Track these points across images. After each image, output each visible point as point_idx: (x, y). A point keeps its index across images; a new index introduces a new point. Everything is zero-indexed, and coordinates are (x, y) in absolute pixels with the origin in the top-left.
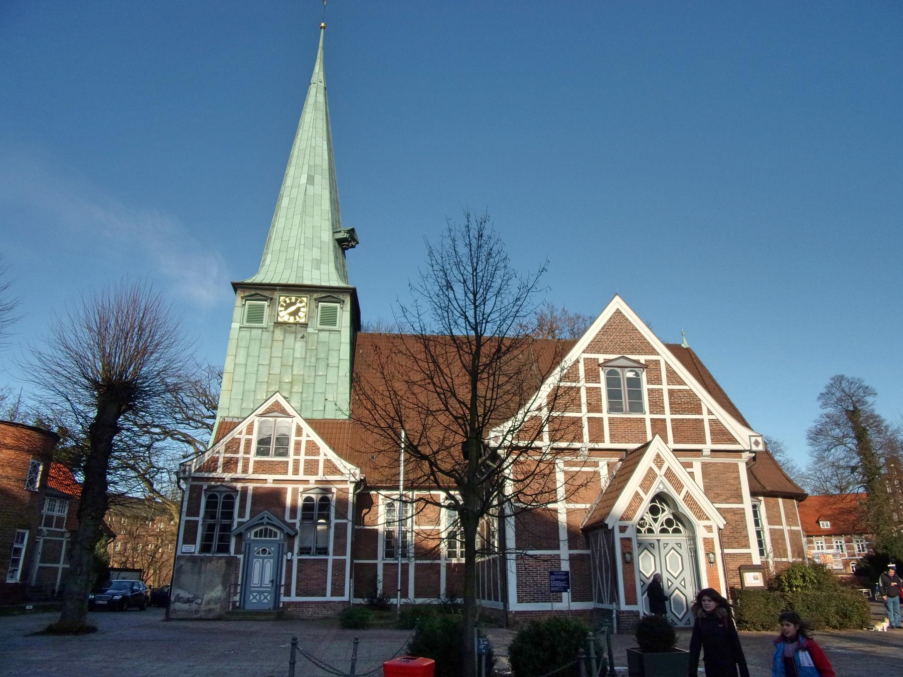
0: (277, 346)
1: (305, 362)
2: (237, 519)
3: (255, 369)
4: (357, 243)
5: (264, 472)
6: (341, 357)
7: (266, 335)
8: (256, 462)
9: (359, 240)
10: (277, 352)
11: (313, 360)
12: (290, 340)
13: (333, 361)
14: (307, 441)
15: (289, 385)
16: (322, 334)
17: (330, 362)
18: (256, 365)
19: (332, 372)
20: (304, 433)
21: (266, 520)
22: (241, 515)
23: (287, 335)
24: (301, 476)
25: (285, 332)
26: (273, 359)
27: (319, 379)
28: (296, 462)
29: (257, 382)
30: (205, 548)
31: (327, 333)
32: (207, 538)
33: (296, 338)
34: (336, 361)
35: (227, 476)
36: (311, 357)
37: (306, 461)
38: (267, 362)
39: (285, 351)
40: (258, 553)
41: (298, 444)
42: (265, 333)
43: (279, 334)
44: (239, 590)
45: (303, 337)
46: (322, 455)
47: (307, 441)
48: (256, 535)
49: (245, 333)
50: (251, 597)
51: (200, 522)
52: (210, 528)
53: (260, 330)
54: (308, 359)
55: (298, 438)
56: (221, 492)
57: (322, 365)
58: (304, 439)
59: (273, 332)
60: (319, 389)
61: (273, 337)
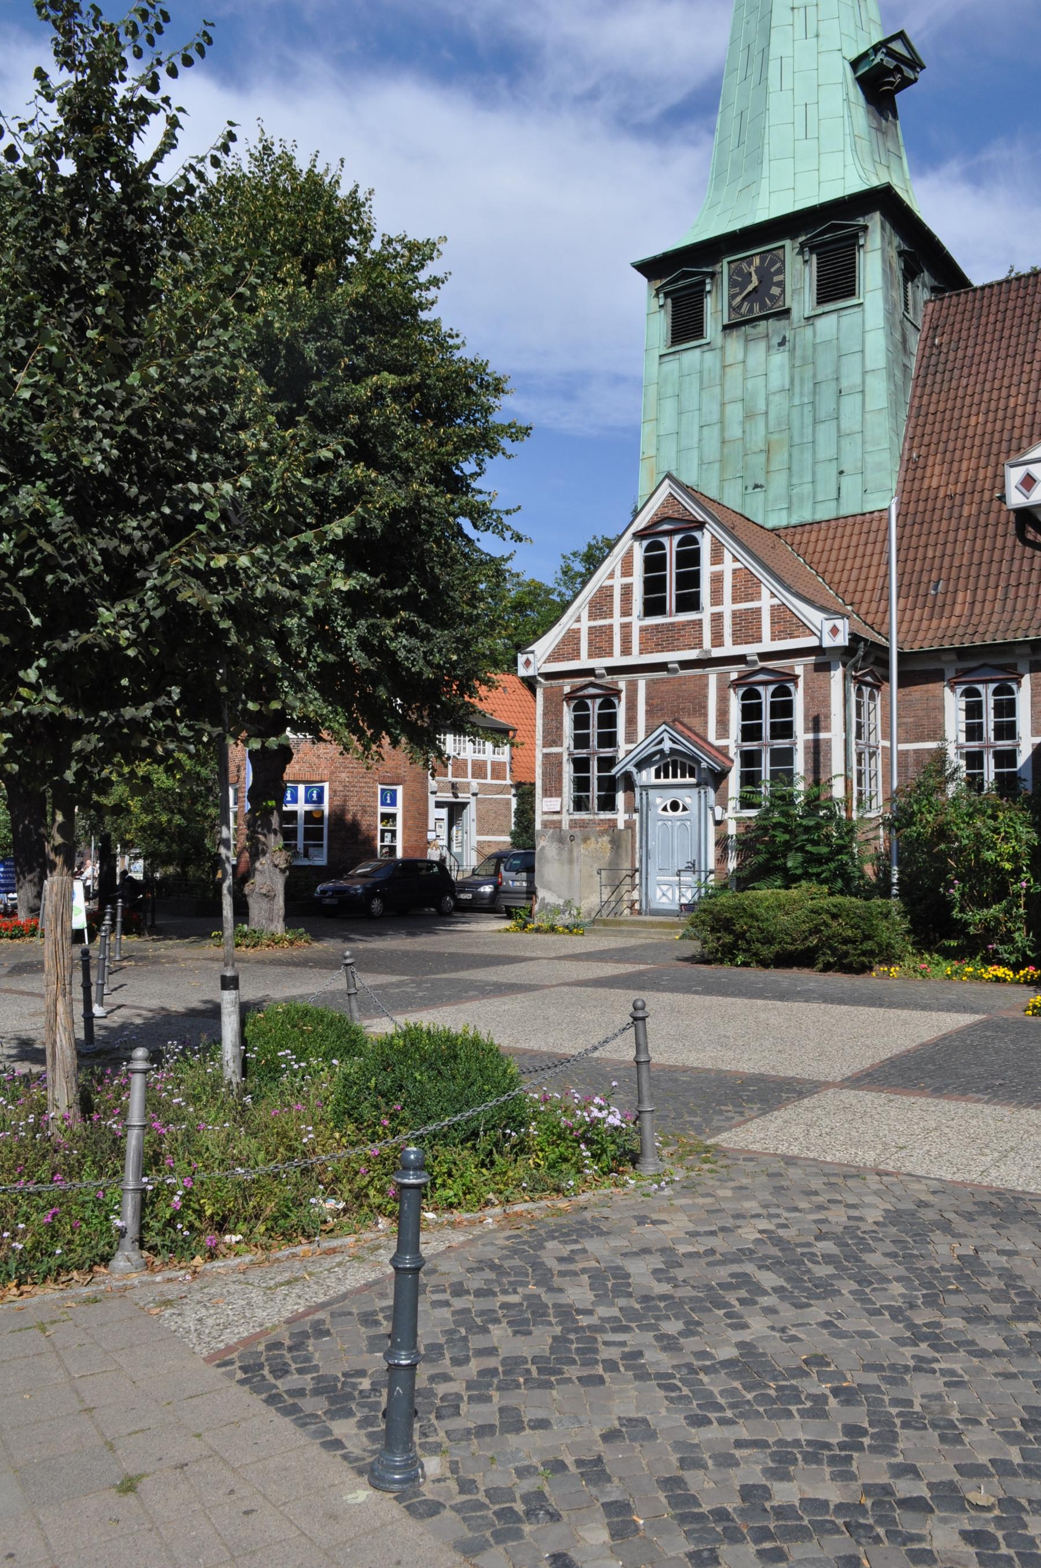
0: (735, 373)
1: (791, 398)
2: (623, 746)
3: (696, 439)
4: (923, 67)
5: (661, 648)
6: (869, 366)
7: (710, 359)
8: (643, 629)
9: (925, 62)
10: (734, 390)
11: (808, 386)
12: (758, 350)
13: (851, 379)
14: (735, 571)
15: (762, 458)
16: (821, 323)
17: (844, 383)
18: (696, 428)
19: (850, 405)
20: (727, 557)
21: (667, 745)
22: (630, 738)
23: (751, 344)
24: (729, 649)
25: (747, 340)
26: (729, 408)
27: (821, 427)
28: (717, 618)
29: (701, 463)
30: (580, 804)
31: (834, 317)
32: (582, 784)
33: (769, 348)
34: (859, 381)
35: (599, 663)
36: (802, 379)
37: (735, 614)
38: (715, 417)
39: (750, 384)
40: (665, 809)
41: (717, 579)
42: (709, 356)
43: (734, 346)
44: (637, 881)
45: (782, 344)
46: (765, 593)
47: (735, 571)
48: (658, 776)
49: (672, 366)
50: (659, 894)
51: (565, 757)
52: (581, 765)
53: (698, 351)
54: (797, 389)
55: (717, 568)
56: (593, 697)
57: (828, 392)
58: (728, 566)
59: (723, 348)
60: (826, 449)
61: (723, 360)
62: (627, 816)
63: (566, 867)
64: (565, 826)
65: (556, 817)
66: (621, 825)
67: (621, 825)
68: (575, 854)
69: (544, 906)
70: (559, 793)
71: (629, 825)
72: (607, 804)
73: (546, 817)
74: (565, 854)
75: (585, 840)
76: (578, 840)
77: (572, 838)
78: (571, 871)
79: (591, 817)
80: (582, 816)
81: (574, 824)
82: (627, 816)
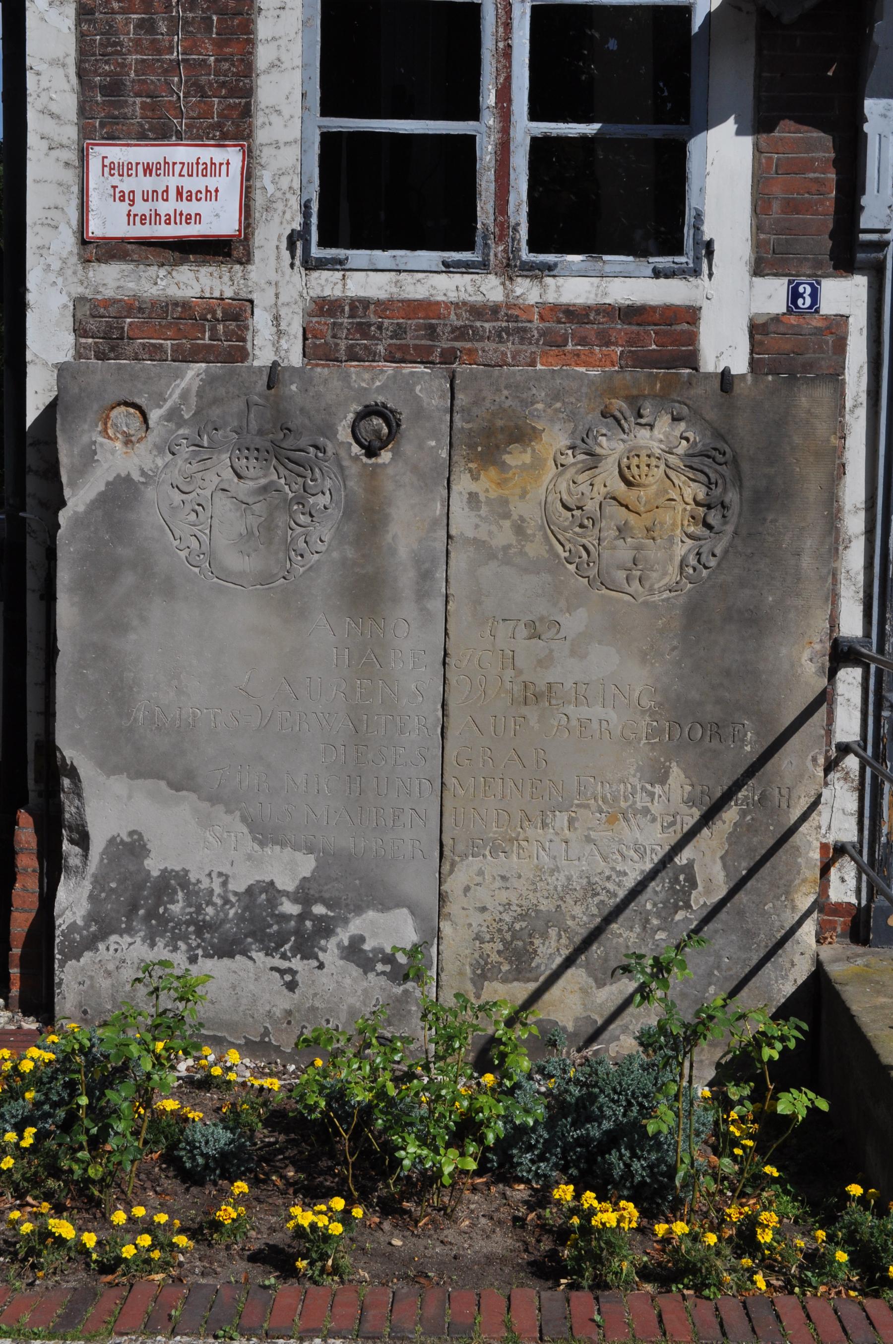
30: (382, 194)
62: (772, 297)
63: (326, 633)
64: (277, 339)
65: (193, 282)
66: (724, 347)
67: (724, 347)
68: (406, 530)
69: (143, 899)
70: (230, 117)
71: (791, 352)
72: (618, 200)
73: (112, 279)
74: (323, 538)
75: (493, 440)
76: (423, 443)
77: (379, 428)
78: (368, 661)
79: (491, 288)
80: (375, 276)
81: (340, 333)
82: (772, 297)
